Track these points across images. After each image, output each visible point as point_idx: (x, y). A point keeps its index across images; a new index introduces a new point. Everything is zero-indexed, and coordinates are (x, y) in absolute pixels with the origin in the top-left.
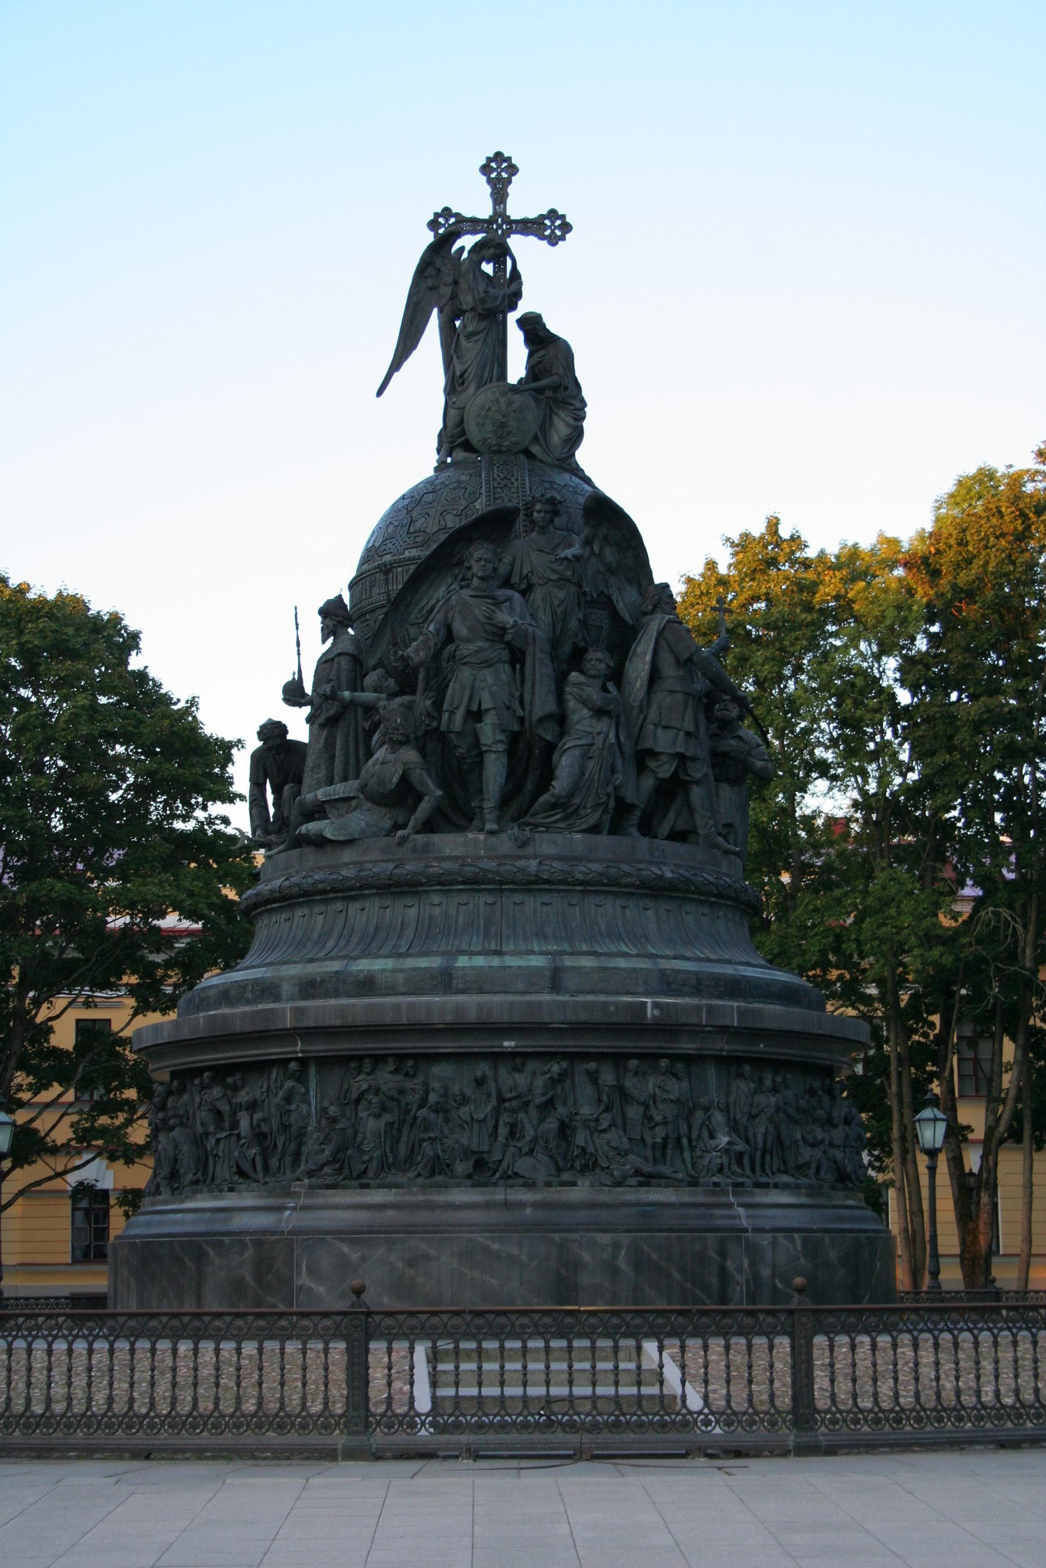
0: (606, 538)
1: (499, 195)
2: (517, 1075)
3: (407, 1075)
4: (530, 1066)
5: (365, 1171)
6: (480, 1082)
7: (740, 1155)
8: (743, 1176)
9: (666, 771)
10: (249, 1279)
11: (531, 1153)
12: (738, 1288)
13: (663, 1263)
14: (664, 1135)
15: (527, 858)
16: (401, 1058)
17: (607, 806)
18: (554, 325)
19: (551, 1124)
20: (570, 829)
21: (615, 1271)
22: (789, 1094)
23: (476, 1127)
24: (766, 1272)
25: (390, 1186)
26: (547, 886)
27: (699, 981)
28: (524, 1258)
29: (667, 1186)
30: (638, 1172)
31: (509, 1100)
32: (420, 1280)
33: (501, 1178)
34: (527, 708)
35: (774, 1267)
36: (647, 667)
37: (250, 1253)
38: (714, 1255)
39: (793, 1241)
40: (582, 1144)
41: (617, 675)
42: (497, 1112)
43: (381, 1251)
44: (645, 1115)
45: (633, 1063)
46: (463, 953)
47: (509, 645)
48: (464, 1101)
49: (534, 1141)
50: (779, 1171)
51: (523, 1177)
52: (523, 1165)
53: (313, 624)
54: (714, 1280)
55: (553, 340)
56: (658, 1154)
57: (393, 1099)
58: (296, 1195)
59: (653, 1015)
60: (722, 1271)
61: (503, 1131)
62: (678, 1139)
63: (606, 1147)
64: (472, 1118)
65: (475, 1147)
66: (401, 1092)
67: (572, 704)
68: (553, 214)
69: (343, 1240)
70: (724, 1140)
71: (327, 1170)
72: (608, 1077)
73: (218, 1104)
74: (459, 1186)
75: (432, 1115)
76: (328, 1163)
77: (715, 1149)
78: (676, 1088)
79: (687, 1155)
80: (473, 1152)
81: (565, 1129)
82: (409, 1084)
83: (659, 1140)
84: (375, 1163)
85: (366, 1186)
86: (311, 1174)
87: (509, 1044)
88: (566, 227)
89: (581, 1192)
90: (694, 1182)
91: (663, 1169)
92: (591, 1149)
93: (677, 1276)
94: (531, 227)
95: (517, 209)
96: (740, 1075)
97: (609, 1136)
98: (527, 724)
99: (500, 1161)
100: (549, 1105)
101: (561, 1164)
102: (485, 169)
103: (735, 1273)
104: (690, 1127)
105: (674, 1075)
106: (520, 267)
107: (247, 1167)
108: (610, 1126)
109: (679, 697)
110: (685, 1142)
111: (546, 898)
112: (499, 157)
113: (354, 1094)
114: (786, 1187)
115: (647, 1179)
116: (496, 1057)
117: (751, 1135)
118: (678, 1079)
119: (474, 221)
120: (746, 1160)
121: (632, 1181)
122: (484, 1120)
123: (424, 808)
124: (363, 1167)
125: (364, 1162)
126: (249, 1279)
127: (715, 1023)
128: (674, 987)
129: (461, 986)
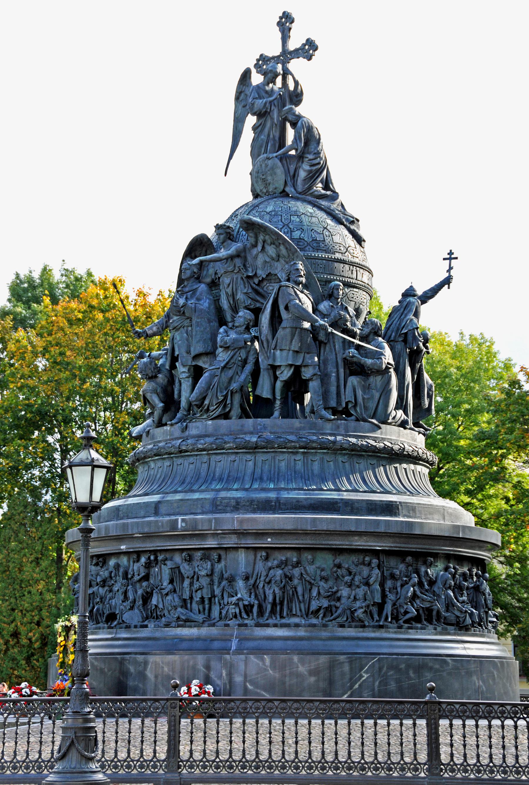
0: (264, 242)
1: (285, 38)
9: (285, 374)
19: (140, 592)
24: (238, 679)
26: (189, 453)
27: (238, 503)
28: (106, 670)
29: (195, 626)
33: (119, 624)
35: (245, 676)
38: (202, 668)
39: (263, 660)
49: (134, 601)
52: (126, 617)
59: (182, 526)
92: (161, 606)
97: (169, 598)
103: (216, 679)
106: (297, 78)
111: (191, 459)
128: (220, 508)
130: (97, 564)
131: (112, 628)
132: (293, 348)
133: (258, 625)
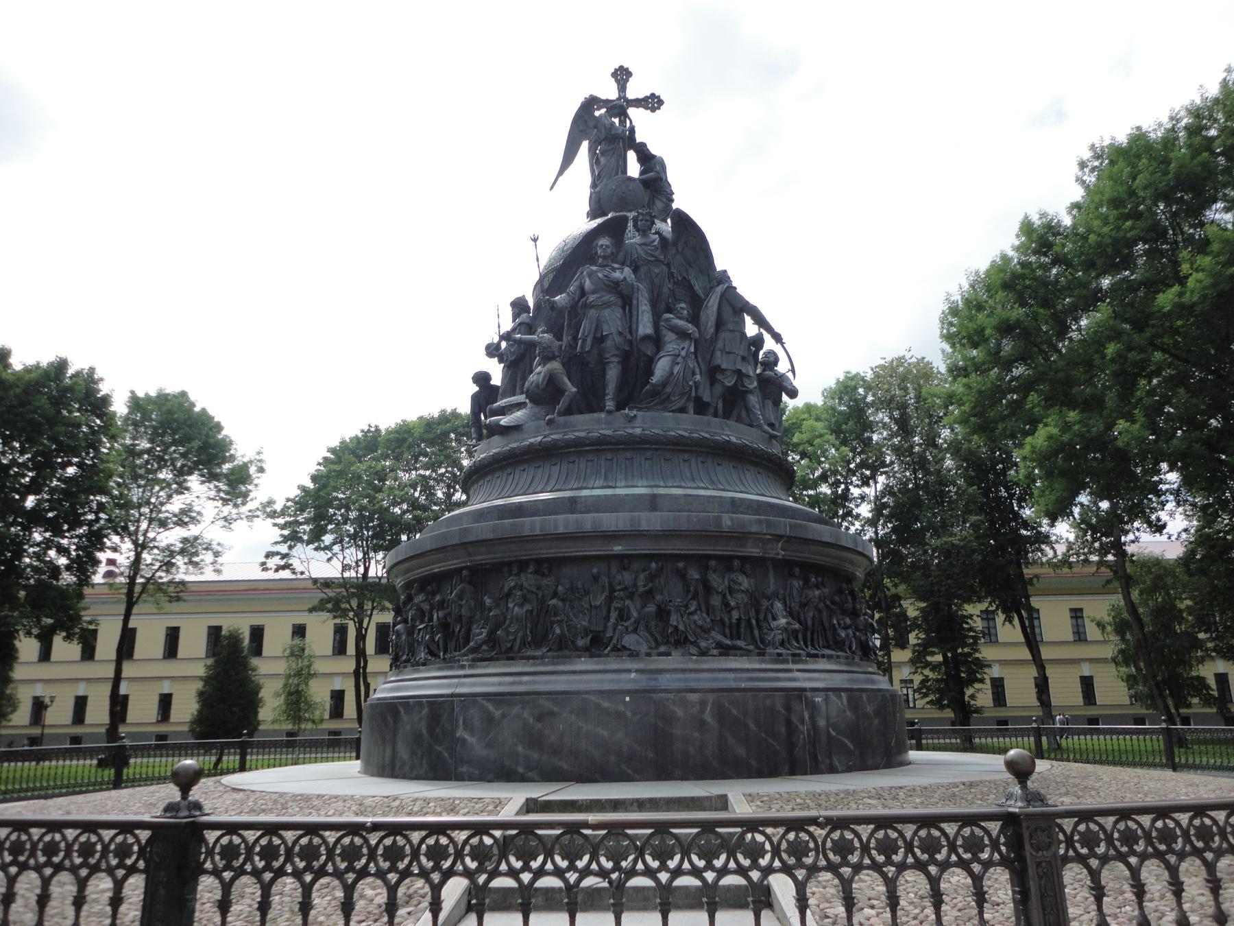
1: (622, 88)
2: (625, 573)
3: (543, 575)
4: (636, 566)
5: (511, 647)
6: (596, 578)
7: (796, 632)
8: (799, 648)
9: (730, 382)
11: (635, 631)
12: (802, 736)
13: (741, 717)
14: (737, 617)
15: (633, 428)
16: (539, 562)
17: (690, 395)
18: (654, 149)
19: (651, 608)
20: (666, 409)
21: (702, 723)
22: (826, 590)
23: (594, 612)
24: (822, 723)
25: (528, 658)
28: (629, 714)
29: (742, 655)
30: (719, 645)
31: (619, 591)
32: (546, 732)
33: (612, 650)
34: (634, 334)
36: (715, 314)
37: (425, 711)
39: (840, 697)
40: (675, 623)
41: (694, 319)
42: (610, 599)
43: (516, 710)
44: (723, 602)
45: (713, 563)
46: (585, 488)
48: (587, 592)
49: (637, 622)
50: (824, 647)
51: (630, 650)
52: (630, 640)
53: (507, 313)
54: (783, 730)
55: (653, 157)
56: (734, 631)
57: (533, 592)
58: (463, 667)
60: (789, 723)
61: (614, 615)
62: (749, 621)
63: (693, 626)
65: (593, 628)
67: (664, 331)
68: (653, 95)
69: (489, 701)
70: (783, 621)
71: (484, 647)
72: (694, 574)
73: (422, 605)
74: (580, 657)
75: (560, 604)
76: (484, 642)
77: (778, 628)
78: (745, 583)
79: (756, 632)
80: (592, 632)
81: (663, 613)
82: (545, 582)
83: (734, 621)
84: (518, 640)
85: (512, 659)
86: (473, 650)
87: (618, 549)
88: (661, 102)
90: (761, 654)
91: (740, 643)
92: (681, 627)
93: (752, 726)
94: (638, 103)
95: (633, 92)
96: (792, 575)
97: (696, 617)
98: (635, 344)
99: (612, 637)
100: (650, 594)
101: (659, 638)
102: (614, 75)
103: (798, 724)
104: (757, 612)
105: (744, 573)
107: (433, 647)
108: (696, 610)
109: (738, 335)
110: (754, 622)
112: (621, 68)
113: (506, 590)
114: (830, 657)
115: (725, 651)
116: (609, 558)
117: (802, 618)
118: (747, 576)
119: (607, 101)
120: (800, 636)
121: (715, 652)
122: (599, 606)
124: (509, 645)
125: (510, 641)
126: (425, 732)
127: (773, 532)
129: (583, 509)
130: (536, 572)
131: (599, 656)
132: (742, 353)
133: (809, 655)
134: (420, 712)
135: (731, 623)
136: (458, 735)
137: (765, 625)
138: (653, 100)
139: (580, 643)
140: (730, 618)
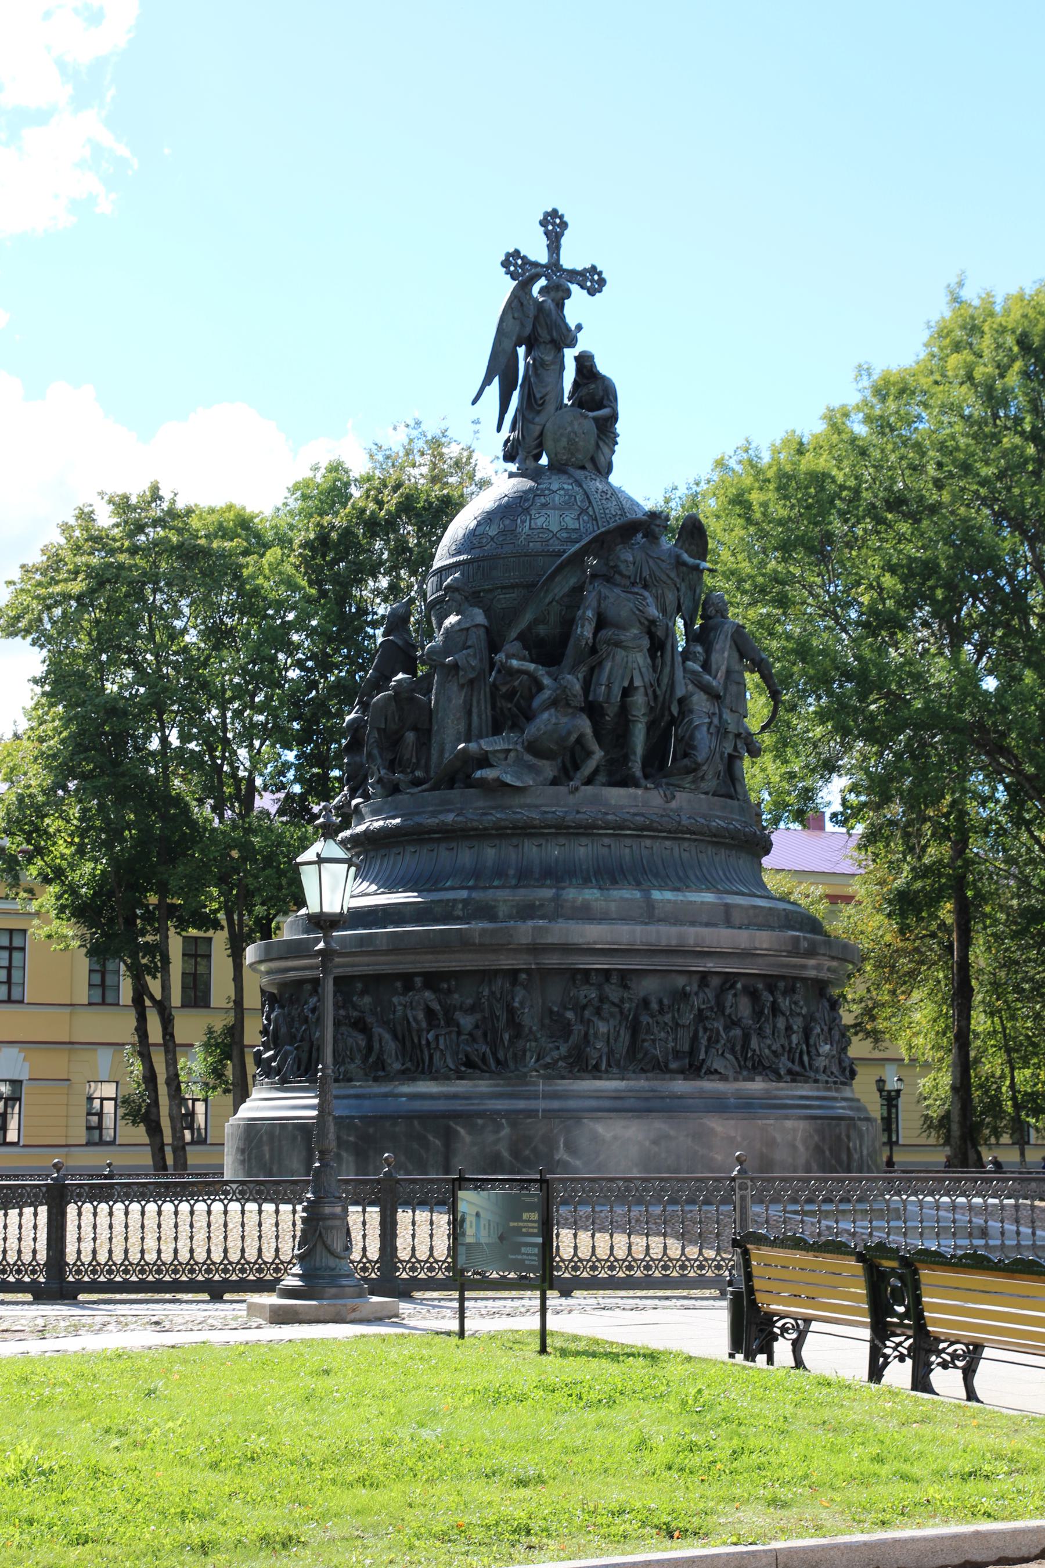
1: (554, 245)
10: (505, 1154)
18: (603, 367)
21: (794, 1147)
23: (680, 1032)
28: (739, 1139)
47: (651, 635)
54: (844, 1157)
63: (767, 1051)
64: (677, 1024)
66: (622, 1000)
71: (560, 1063)
79: (806, 1058)
86: (547, 1066)
88: (602, 282)
89: (757, 1086)
93: (827, 1153)
95: (571, 259)
111: (686, 844)
121: (788, 1078)
123: (591, 765)
126: (505, 1154)
134: (497, 1132)
135: (791, 1048)
136: (557, 1158)
137: (813, 1052)
138: (597, 282)
139: (673, 1065)
140: (790, 1043)
